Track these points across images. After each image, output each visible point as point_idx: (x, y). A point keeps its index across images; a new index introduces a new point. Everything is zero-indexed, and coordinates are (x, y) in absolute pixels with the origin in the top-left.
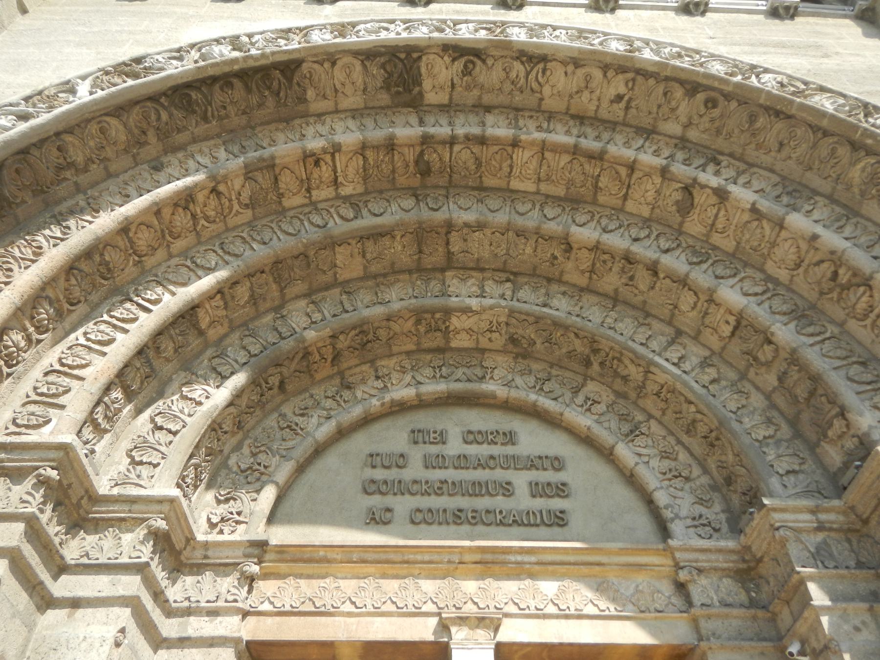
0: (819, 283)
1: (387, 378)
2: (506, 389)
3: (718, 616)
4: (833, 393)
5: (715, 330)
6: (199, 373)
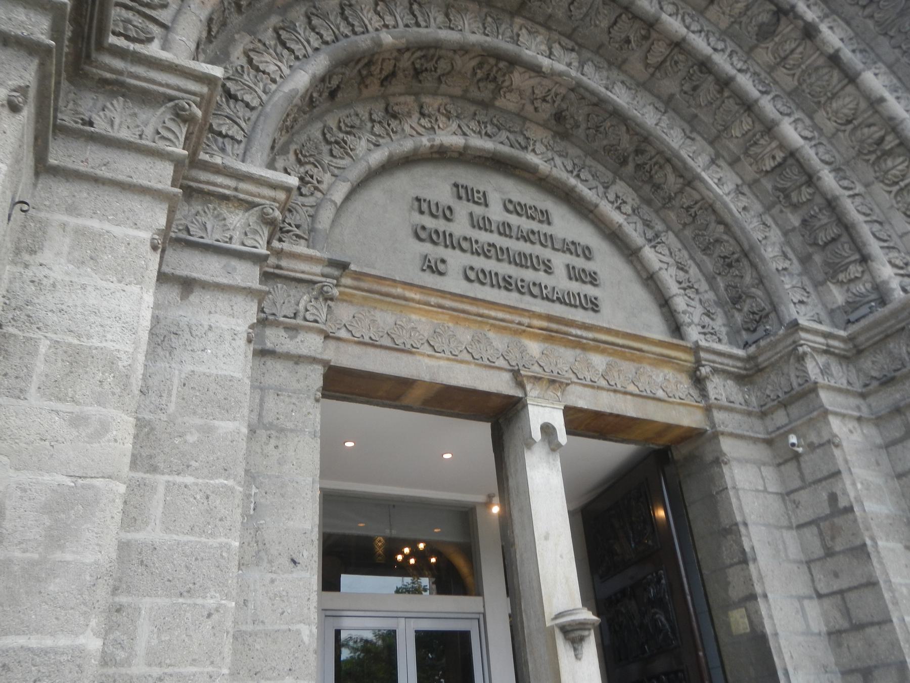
0: (862, 142)
4: (862, 242)
5: (757, 162)
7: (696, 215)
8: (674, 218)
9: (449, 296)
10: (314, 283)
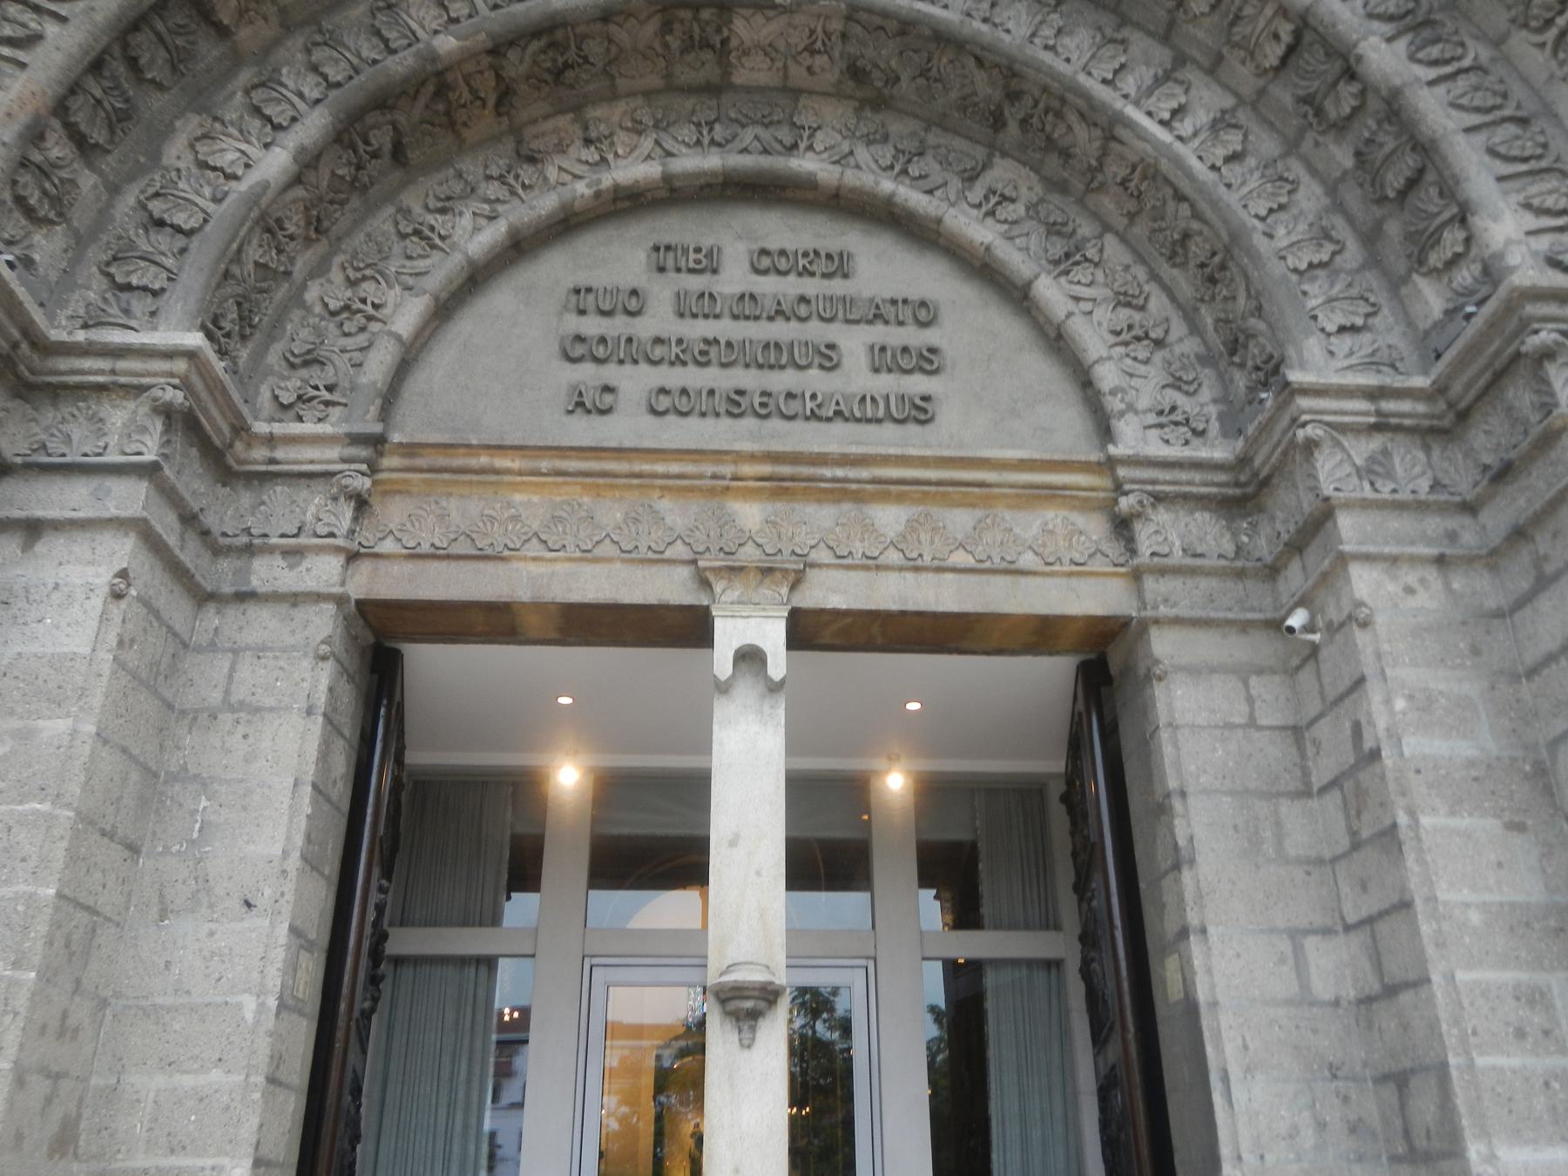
1: (606, 142)
2: (838, 169)
3: (1178, 571)
4: (1454, 176)
5: (1252, 54)
6: (227, 118)
7: (1141, 193)
8: (1112, 207)
9: (573, 453)
10: (332, 474)
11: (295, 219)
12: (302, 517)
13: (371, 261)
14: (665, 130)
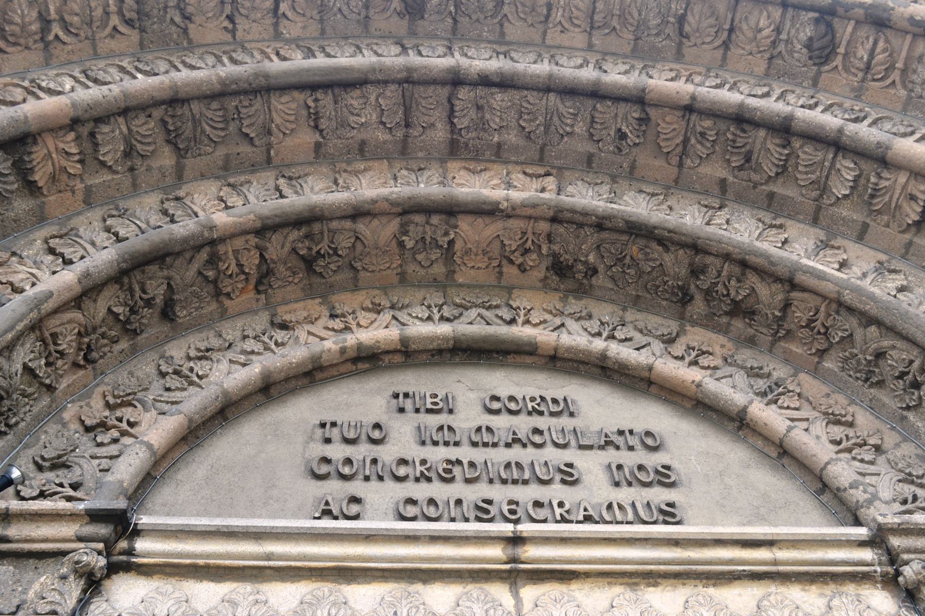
1: (350, 317)
7: (827, 328)
10: (64, 553)
11: (69, 338)
12: (24, 597)
13: (129, 391)
14: (400, 309)
